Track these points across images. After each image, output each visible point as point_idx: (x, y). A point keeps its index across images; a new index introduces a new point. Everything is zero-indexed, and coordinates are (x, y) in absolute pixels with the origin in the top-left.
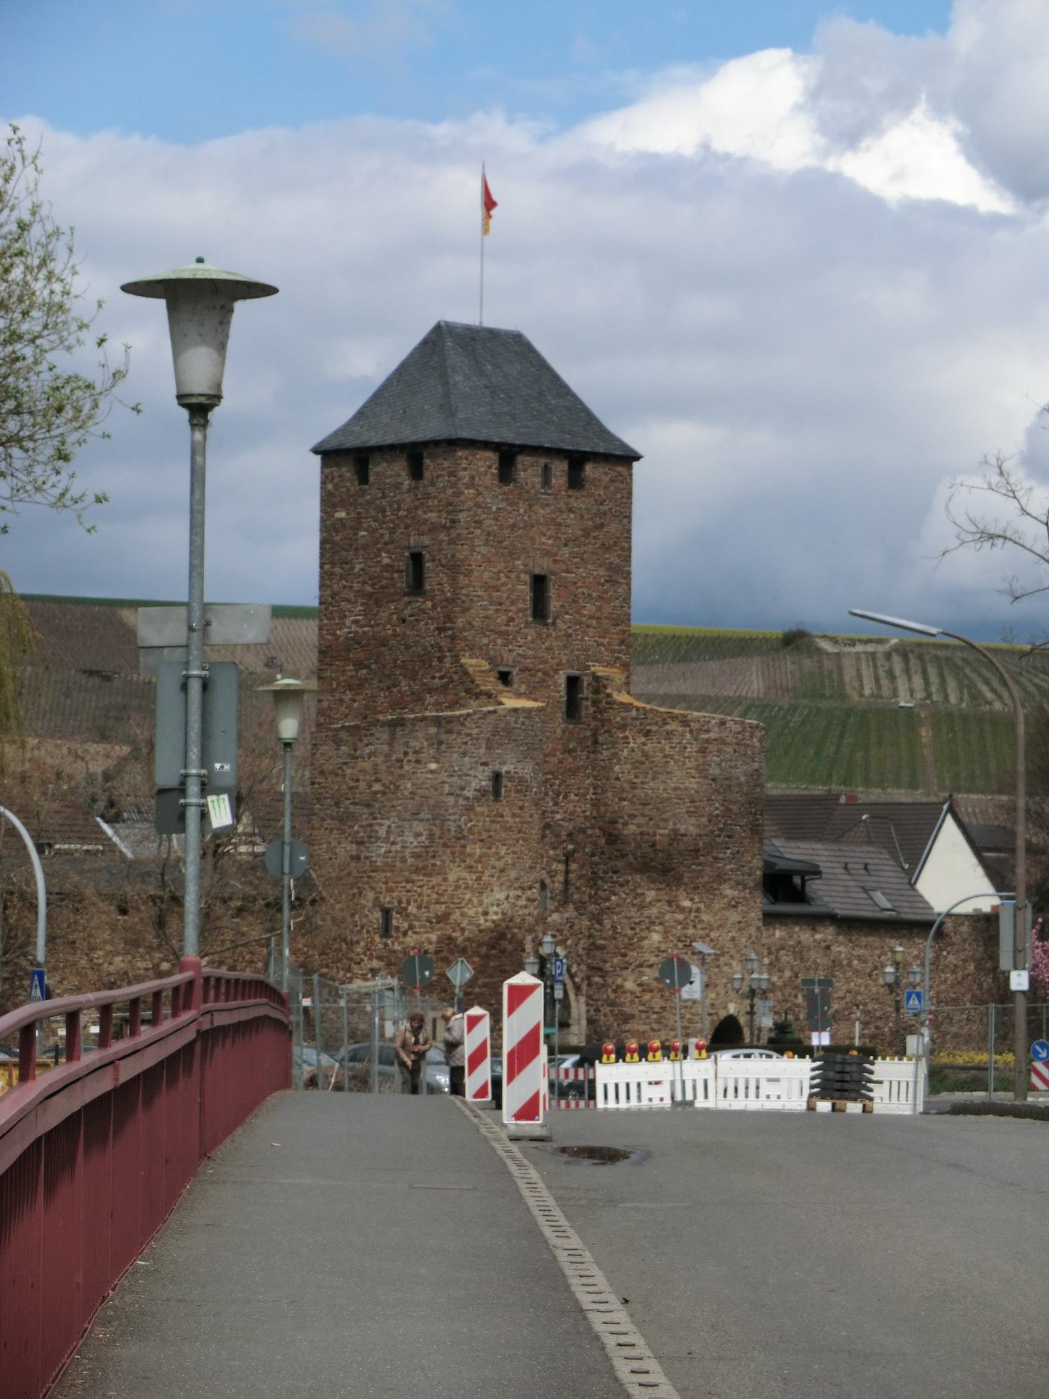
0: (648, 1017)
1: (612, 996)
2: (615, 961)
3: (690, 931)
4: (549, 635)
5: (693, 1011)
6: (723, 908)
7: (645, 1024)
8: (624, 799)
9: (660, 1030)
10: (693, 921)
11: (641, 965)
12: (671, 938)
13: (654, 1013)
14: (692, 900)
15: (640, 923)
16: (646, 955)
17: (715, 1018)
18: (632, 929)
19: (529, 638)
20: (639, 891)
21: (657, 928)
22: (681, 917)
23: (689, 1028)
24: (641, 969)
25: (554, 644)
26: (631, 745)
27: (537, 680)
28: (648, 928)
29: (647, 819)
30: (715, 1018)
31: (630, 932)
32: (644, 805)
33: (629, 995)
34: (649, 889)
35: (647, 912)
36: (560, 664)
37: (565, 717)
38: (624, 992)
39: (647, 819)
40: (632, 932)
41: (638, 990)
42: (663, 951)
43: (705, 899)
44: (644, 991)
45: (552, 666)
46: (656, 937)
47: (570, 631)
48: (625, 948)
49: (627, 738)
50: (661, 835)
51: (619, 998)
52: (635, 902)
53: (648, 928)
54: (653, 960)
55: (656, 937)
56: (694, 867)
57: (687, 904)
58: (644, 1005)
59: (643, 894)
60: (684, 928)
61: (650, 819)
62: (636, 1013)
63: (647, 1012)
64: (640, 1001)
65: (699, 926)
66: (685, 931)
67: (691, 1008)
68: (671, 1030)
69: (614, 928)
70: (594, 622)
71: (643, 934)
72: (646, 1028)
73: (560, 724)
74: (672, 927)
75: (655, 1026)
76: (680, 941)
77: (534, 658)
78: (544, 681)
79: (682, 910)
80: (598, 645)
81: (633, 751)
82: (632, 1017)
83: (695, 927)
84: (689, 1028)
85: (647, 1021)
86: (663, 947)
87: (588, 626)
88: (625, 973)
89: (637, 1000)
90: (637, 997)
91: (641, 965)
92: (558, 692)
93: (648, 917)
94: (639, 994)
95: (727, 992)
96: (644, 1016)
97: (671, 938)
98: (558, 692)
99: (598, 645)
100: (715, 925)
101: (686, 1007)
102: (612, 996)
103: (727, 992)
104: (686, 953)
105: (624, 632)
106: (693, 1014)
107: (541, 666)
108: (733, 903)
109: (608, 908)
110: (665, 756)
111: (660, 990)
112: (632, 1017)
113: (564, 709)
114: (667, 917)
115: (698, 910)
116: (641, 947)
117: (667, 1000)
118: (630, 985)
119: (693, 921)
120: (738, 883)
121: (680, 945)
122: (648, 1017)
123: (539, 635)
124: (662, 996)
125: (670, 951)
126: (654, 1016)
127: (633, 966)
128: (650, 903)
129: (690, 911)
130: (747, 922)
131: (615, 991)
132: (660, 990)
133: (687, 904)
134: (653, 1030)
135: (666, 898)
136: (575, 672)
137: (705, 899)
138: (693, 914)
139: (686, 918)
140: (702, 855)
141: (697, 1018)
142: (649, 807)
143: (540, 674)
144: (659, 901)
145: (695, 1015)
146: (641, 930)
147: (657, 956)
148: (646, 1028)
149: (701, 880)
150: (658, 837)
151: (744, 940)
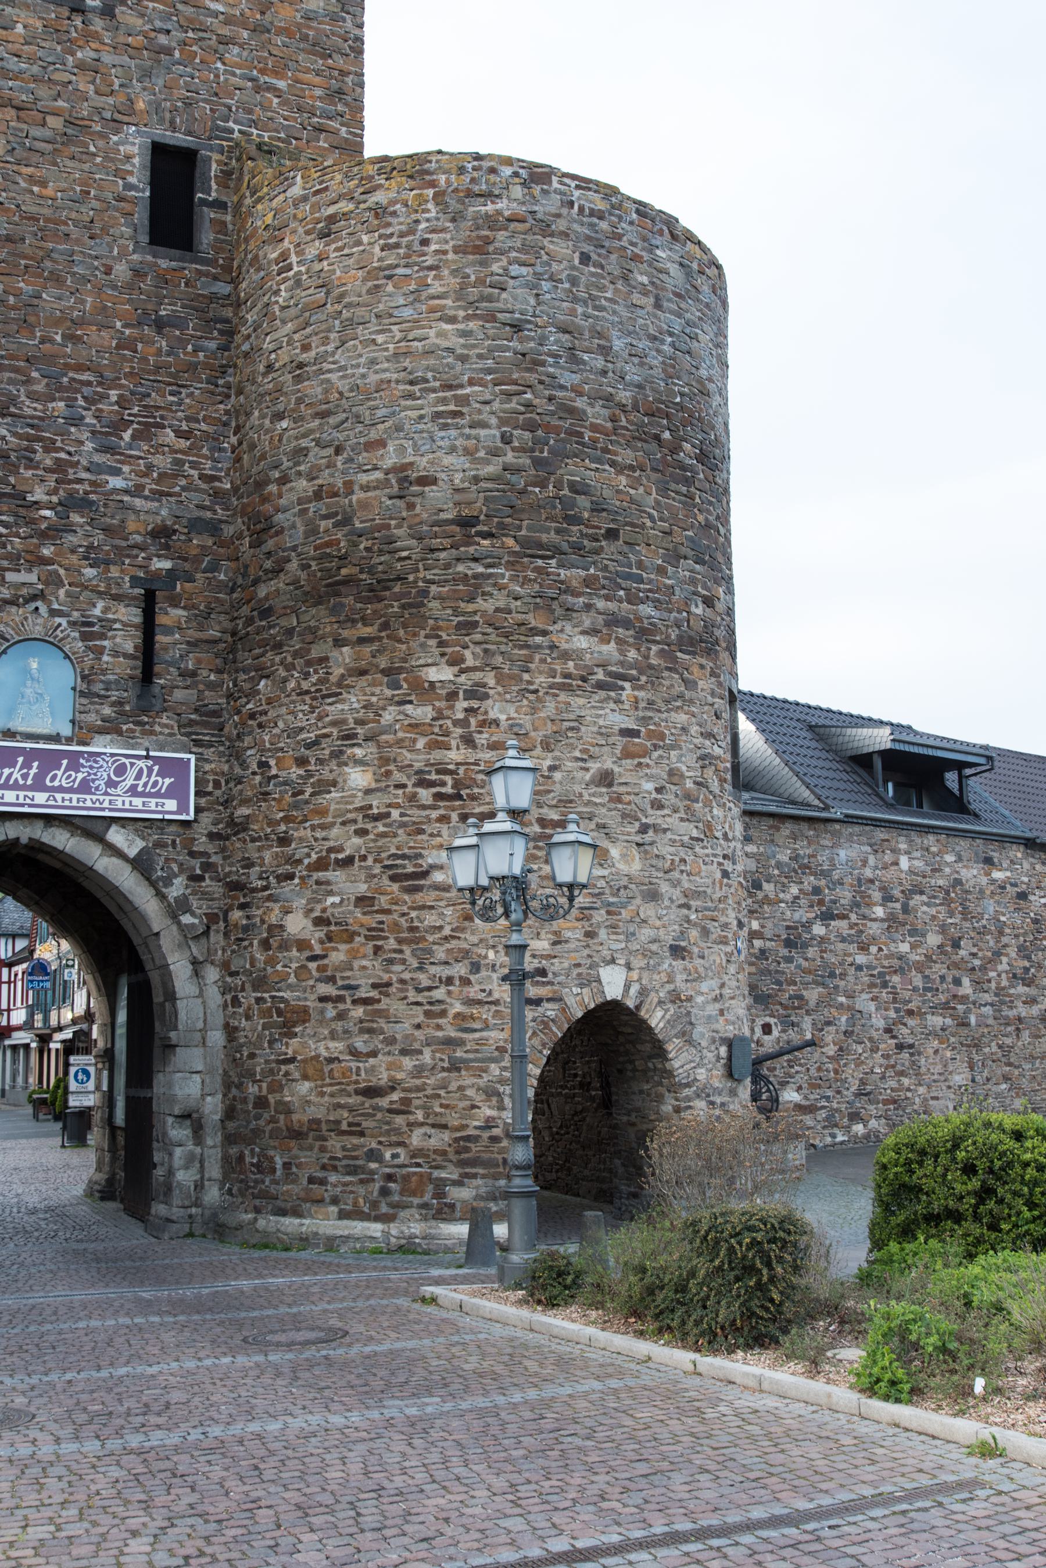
0: (341, 1016)
1: (261, 957)
2: (267, 856)
3: (455, 755)
4: (89, 36)
5: (473, 992)
6: (563, 687)
7: (333, 1035)
8: (279, 416)
9: (374, 1054)
10: (464, 723)
11: (321, 865)
12: (398, 777)
13: (355, 1002)
14: (455, 661)
15: (315, 743)
16: (335, 831)
17: (550, 1010)
18: (302, 762)
19: (19, 28)
20: (315, 653)
21: (359, 752)
22: (423, 713)
23: (461, 1043)
24: (320, 875)
25: (107, 58)
26: (296, 269)
27: (48, 133)
28: (337, 754)
29: (330, 451)
30: (550, 1010)
31: (295, 772)
32: (324, 415)
33: (294, 953)
34: (339, 643)
35: (334, 710)
36: (131, 111)
37: (144, 239)
38: (284, 946)
39: (330, 451)
40: (301, 772)
41: (315, 936)
42: (377, 818)
43: (498, 660)
44: (330, 938)
45: (99, 110)
46: (358, 778)
47: (163, 39)
48: (287, 819)
49: (284, 256)
50: (366, 488)
51: (271, 961)
52: (305, 685)
53: (337, 754)
54: (353, 844)
55: (358, 778)
56: (461, 568)
57: (441, 674)
58: (332, 980)
59: (326, 659)
60: (435, 745)
61: (338, 451)
62: (312, 1003)
63: (340, 999)
64: (321, 969)
65: (481, 739)
66: (437, 755)
67: (466, 982)
68: (404, 1052)
69: (263, 765)
70: (245, 34)
71: (326, 774)
72: (337, 1047)
73: (123, 254)
74: (399, 743)
75: (360, 1043)
76: (423, 783)
77: (35, 79)
78: (68, 140)
79: (426, 691)
80: (257, 89)
81: (298, 283)
82: (303, 1015)
83: (468, 741)
84: (460, 1043)
85: (339, 1026)
86: (377, 804)
87: (225, 41)
88: (288, 888)
89: (313, 965)
90: (314, 958)
91: (321, 865)
92: (117, 173)
93: (334, 723)
94: (318, 950)
95: (590, 935)
96: (331, 1012)
97: (398, 777)
98: (117, 173)
99: (257, 89)
100: (537, 736)
101: (449, 981)
102: (261, 957)
103: (590, 935)
104: (444, 819)
105: (343, 73)
106: (470, 1002)
107: (60, 103)
108: (600, 675)
109: (252, 716)
110: (371, 275)
111: (375, 934)
112: (303, 1015)
113: (141, 215)
114: (388, 716)
115: (477, 693)
116: (323, 812)
117: (391, 962)
118: (297, 924)
119: (464, 723)
120: (613, 621)
121: (425, 795)
122: (341, 1016)
123: (53, 30)
124: (377, 950)
125: (395, 814)
126: (359, 1012)
127: (300, 871)
128: (339, 685)
129: (452, 696)
130: (651, 735)
131: (266, 945)
132: (375, 934)
133: (441, 674)
134: (354, 1053)
135: (383, 662)
136: (180, 139)
137: (498, 660)
138: (462, 704)
139: (439, 716)
140: (489, 535)
141: (486, 1013)
142: (332, 420)
143: (52, 121)
144: (363, 673)
145: (479, 1002)
146: (320, 761)
147: (362, 833)
148: (337, 1047)
149: (481, 604)
150: (358, 496)
151: (649, 786)
